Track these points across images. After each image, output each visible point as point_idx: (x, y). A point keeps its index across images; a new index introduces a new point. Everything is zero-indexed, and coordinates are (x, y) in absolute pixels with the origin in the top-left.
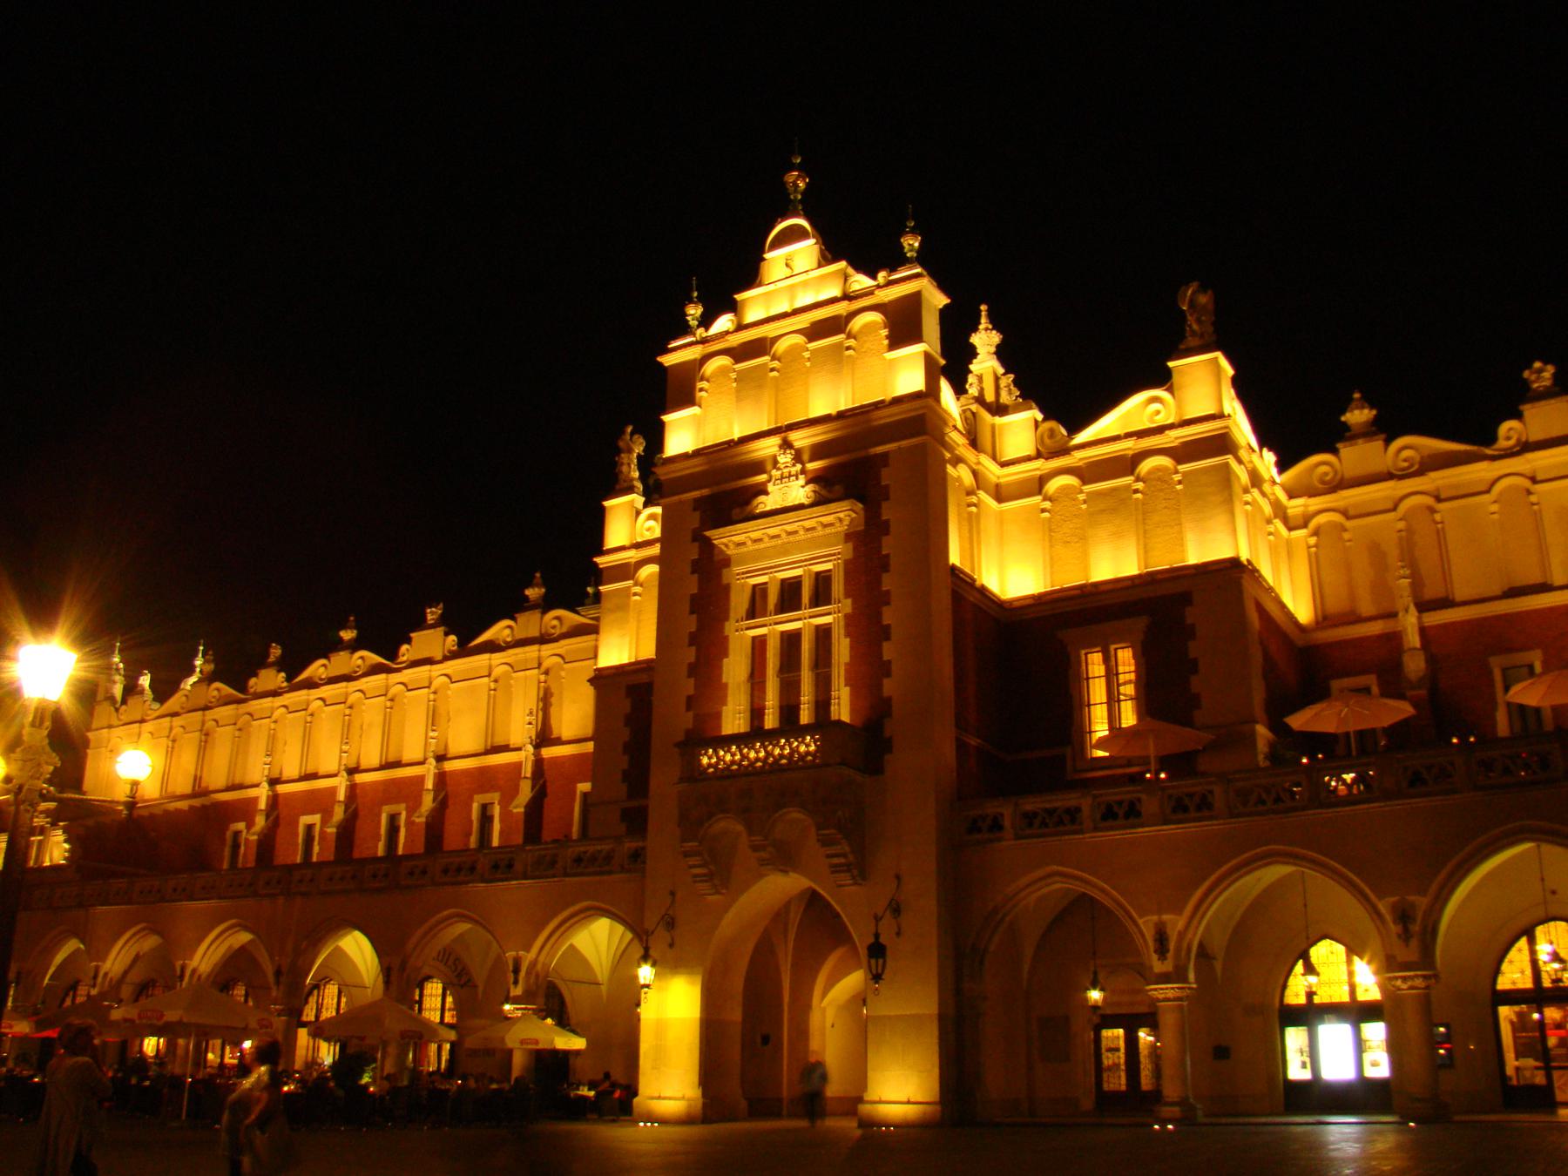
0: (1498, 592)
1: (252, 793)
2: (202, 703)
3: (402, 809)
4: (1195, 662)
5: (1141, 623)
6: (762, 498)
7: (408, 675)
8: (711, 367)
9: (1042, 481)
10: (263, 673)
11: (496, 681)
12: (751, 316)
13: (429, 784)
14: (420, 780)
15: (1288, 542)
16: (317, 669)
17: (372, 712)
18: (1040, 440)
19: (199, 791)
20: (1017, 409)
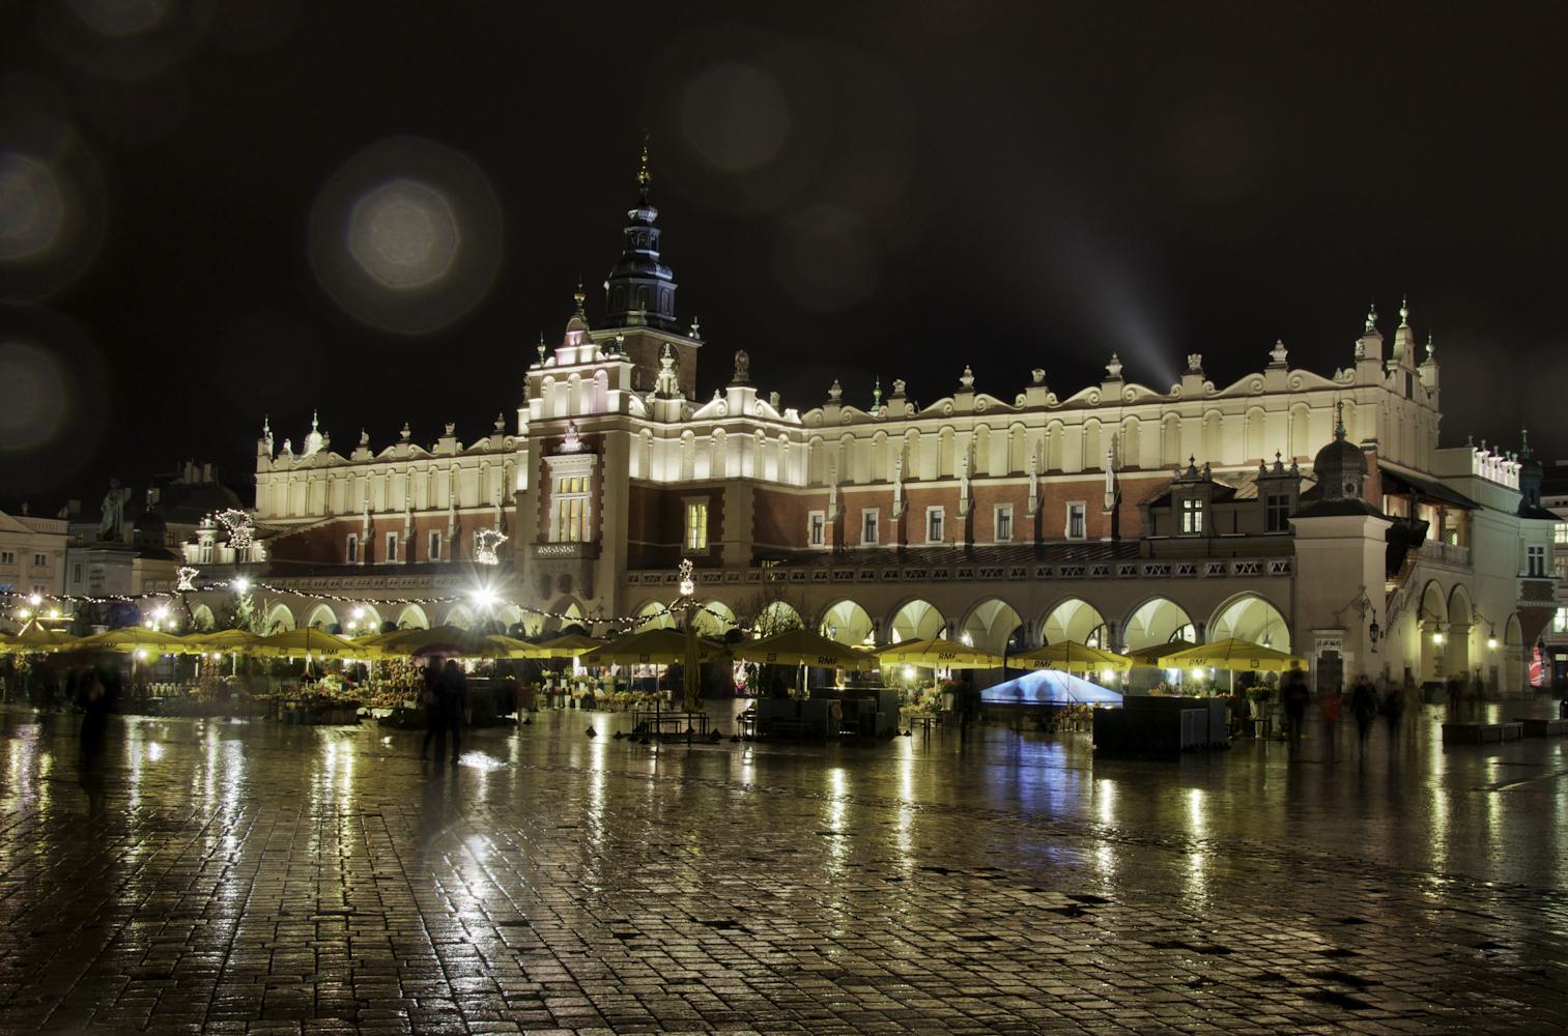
0: (868, 481)
1: (359, 518)
2: (325, 463)
3: (439, 532)
4: (723, 516)
5: (707, 498)
6: (563, 445)
7: (438, 462)
8: (548, 379)
9: (682, 431)
10: (359, 450)
11: (482, 469)
12: (561, 362)
13: (451, 522)
14: (447, 518)
15: (801, 448)
16: (389, 451)
17: (421, 479)
18: (682, 413)
19: (329, 515)
20: (678, 397)
